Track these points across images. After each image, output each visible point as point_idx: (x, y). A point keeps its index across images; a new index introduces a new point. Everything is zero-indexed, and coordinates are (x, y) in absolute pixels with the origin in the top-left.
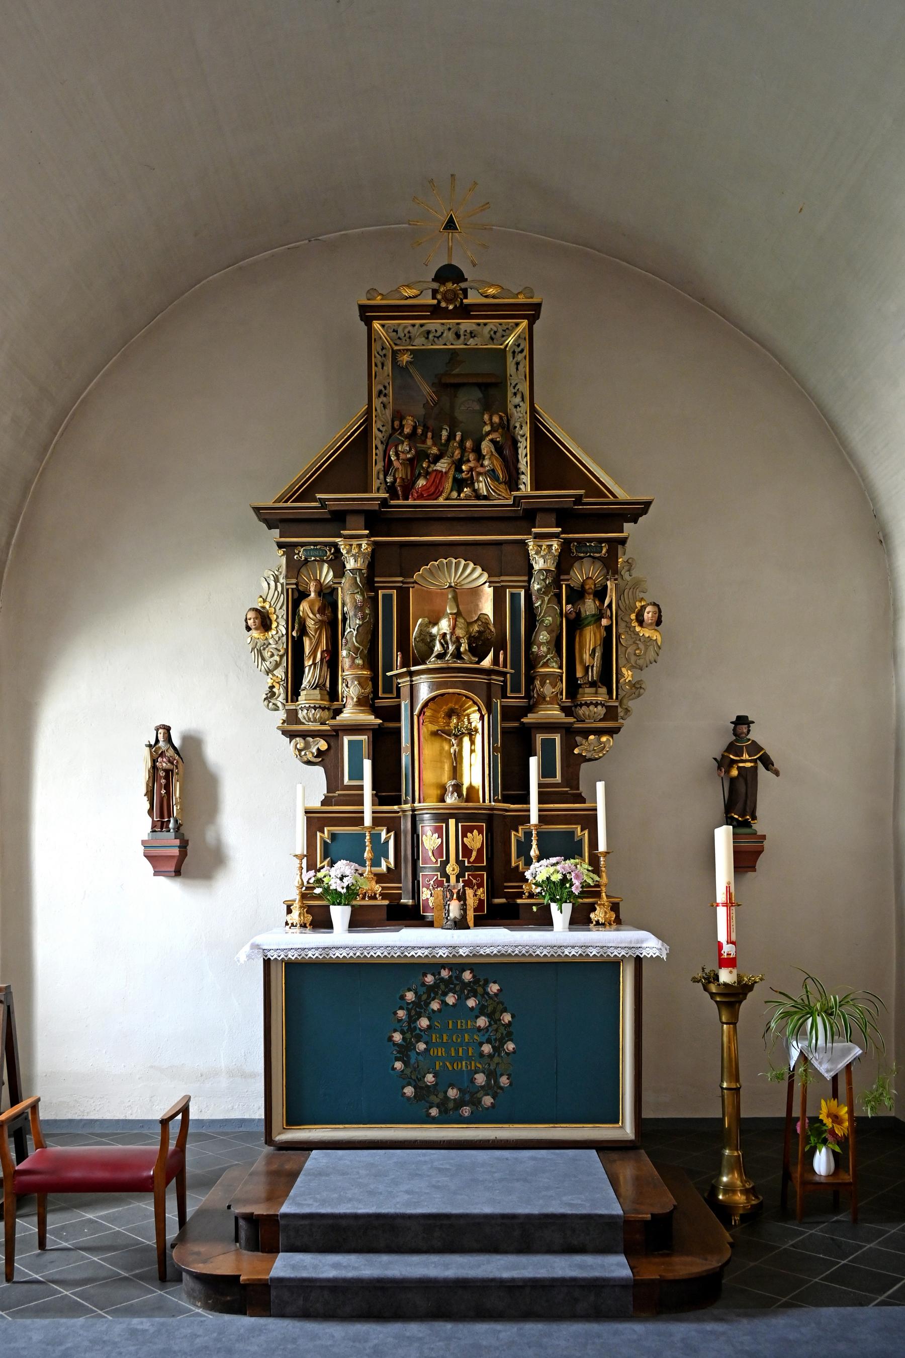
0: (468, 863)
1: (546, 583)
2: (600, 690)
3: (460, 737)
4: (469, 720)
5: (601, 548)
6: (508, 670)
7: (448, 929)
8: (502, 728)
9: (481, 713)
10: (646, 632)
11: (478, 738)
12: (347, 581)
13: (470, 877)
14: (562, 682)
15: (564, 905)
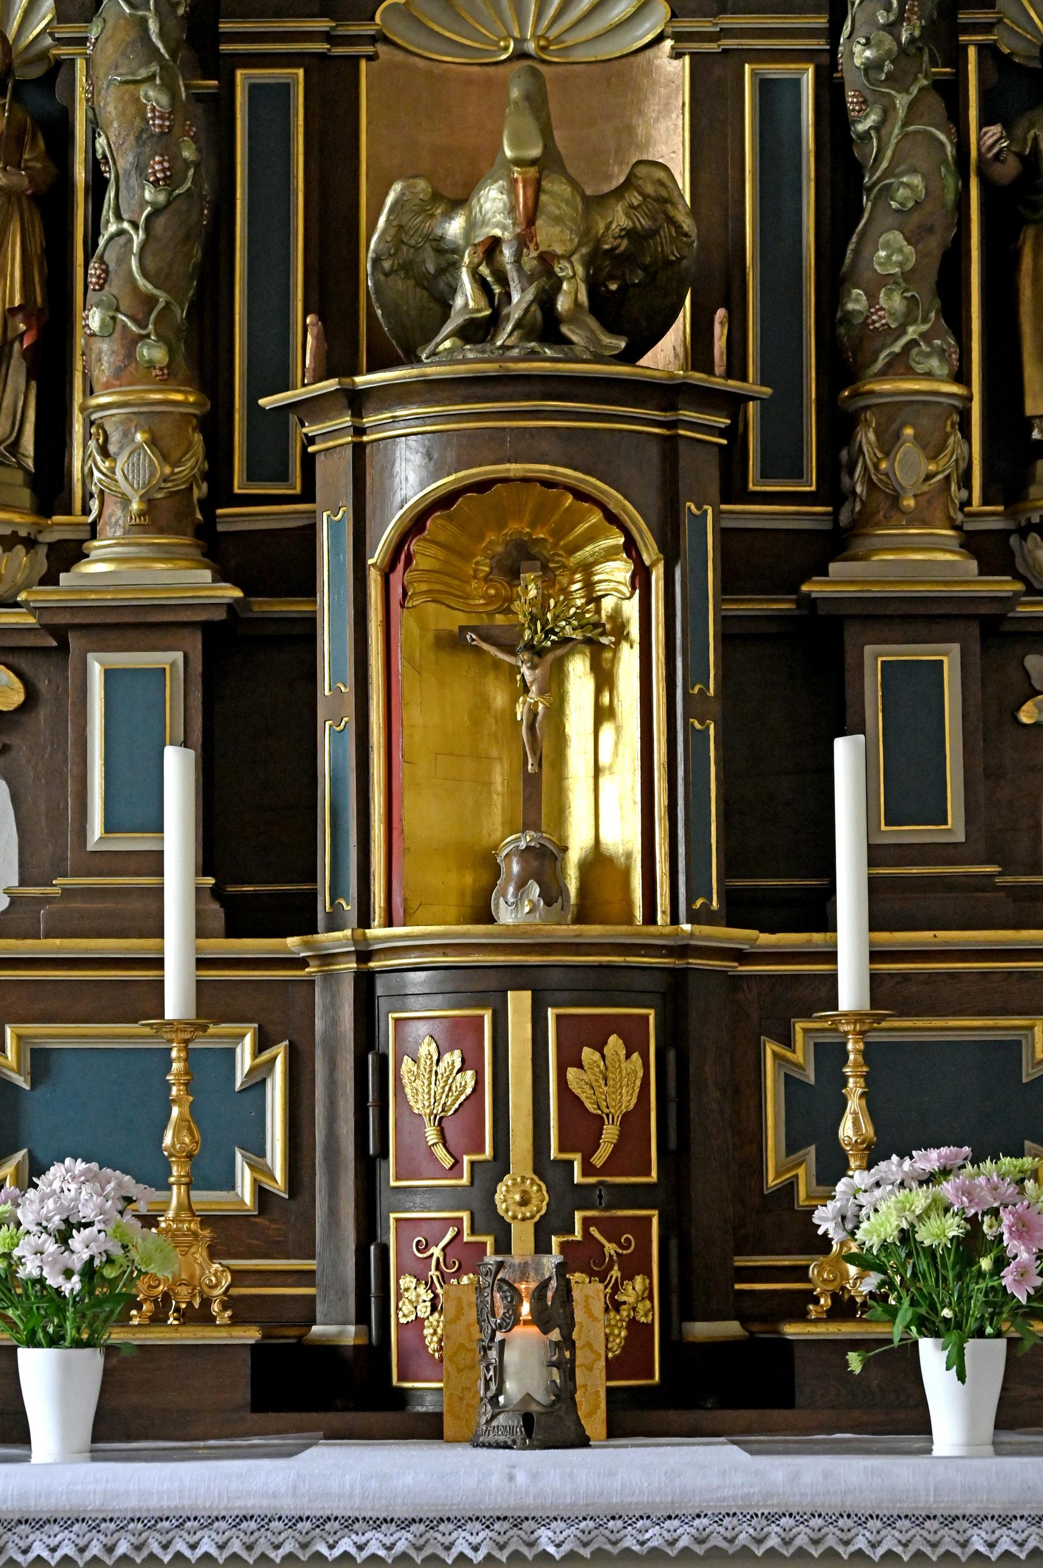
0: (585, 1173)
1: (898, 40)
3: (550, 658)
4: (589, 585)
6: (752, 385)
7: (499, 1446)
8: (723, 620)
9: (638, 562)
11: (628, 660)
12: (108, 31)
13: (593, 1230)
14: (967, 436)
15: (971, 1346)
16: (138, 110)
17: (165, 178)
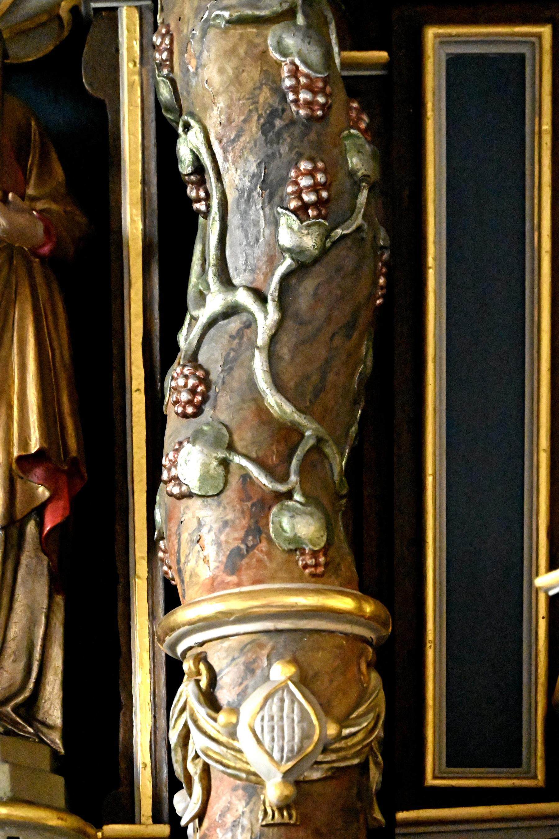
16: (265, 72)
17: (319, 204)
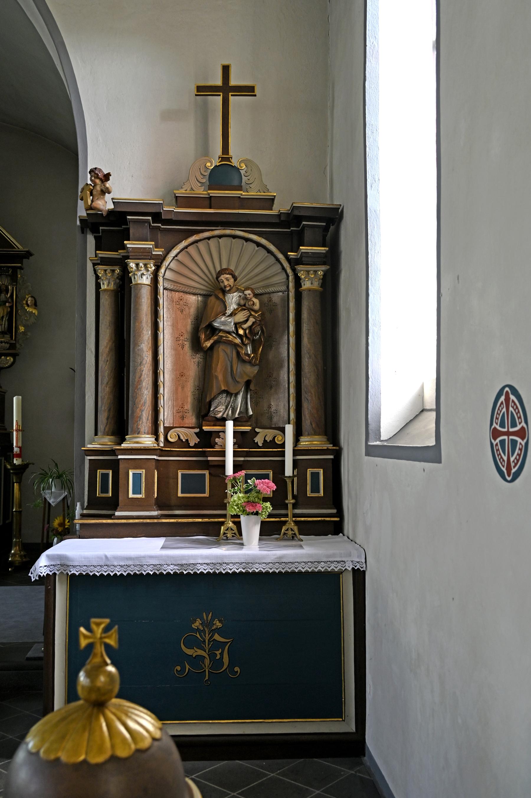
2: (6, 336)
5: (9, 271)
10: (29, 309)
